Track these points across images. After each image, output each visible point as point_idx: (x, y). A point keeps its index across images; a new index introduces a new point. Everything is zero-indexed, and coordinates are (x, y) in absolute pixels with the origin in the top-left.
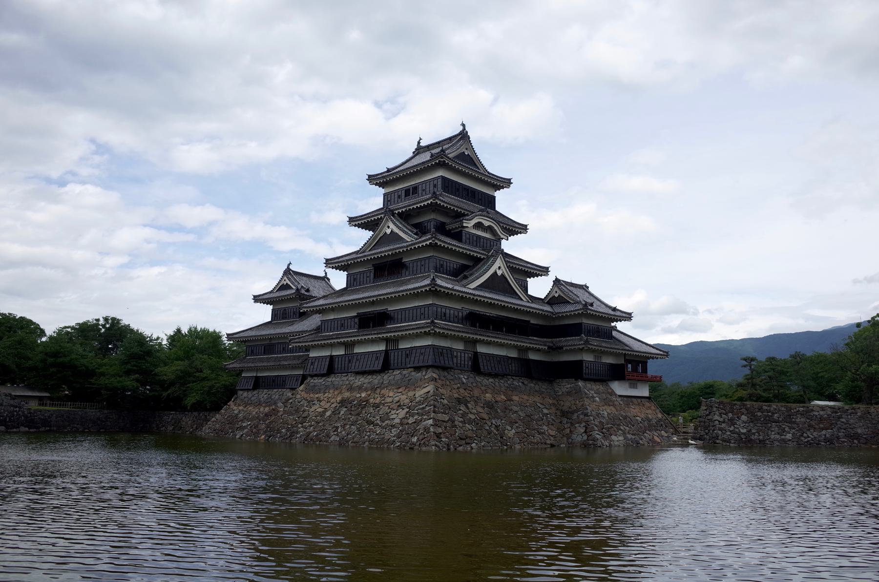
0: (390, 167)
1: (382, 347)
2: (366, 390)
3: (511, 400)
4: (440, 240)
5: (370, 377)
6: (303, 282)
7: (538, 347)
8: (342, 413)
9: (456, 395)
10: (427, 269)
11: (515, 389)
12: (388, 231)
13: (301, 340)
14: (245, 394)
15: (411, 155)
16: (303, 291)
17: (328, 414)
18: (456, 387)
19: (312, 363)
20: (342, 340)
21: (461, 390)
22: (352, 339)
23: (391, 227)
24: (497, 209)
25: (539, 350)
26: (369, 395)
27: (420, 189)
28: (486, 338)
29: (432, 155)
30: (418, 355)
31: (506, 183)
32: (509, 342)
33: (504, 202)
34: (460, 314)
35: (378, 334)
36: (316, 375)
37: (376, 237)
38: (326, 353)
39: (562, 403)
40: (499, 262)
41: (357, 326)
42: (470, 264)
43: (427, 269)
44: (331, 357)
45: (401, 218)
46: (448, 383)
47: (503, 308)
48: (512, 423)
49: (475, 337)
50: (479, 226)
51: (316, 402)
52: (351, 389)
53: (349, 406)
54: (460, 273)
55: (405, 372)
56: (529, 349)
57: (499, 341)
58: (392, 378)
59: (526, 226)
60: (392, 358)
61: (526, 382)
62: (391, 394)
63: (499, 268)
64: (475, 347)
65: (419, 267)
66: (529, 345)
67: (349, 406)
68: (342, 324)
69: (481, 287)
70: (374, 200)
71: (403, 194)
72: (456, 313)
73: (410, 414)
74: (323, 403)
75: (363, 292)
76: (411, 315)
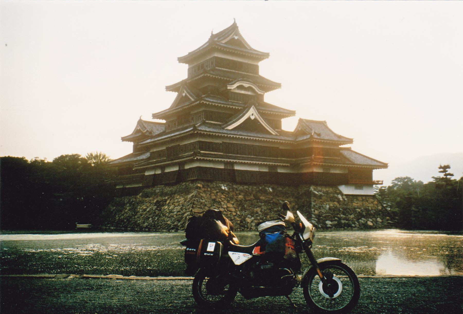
3: (259, 199)
4: (205, 100)
9: (214, 197)
12: (184, 94)
14: (118, 199)
18: (215, 192)
21: (218, 194)
25: (288, 166)
28: (238, 161)
31: (263, 56)
38: (152, 173)
39: (300, 200)
44: (155, 175)
46: (209, 189)
48: (252, 214)
50: (240, 87)
55: (187, 183)
56: (277, 165)
62: (178, 198)
63: (253, 115)
64: (233, 167)
68: (160, 154)
73: (182, 209)
74: (147, 204)
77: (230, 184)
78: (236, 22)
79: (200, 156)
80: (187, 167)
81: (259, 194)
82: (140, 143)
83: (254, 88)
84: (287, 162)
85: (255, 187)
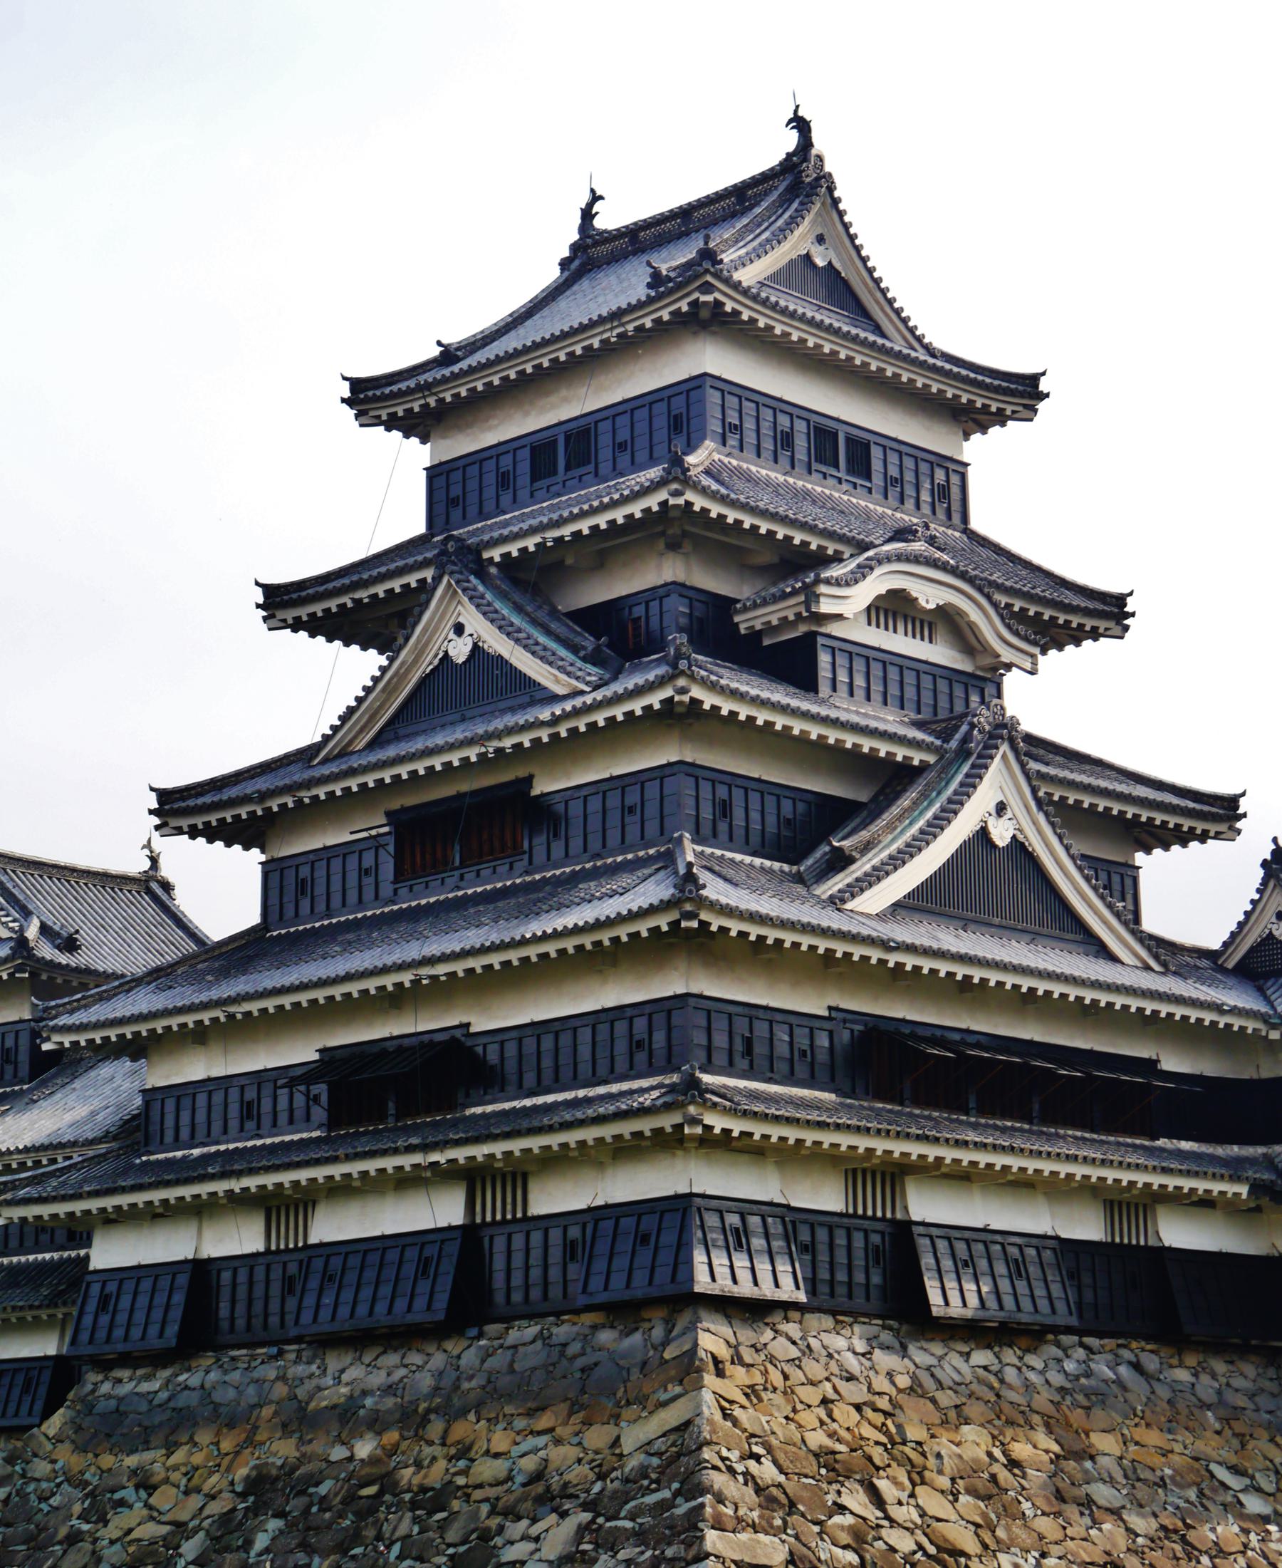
0: (454, 336)
1: (445, 1210)
2: (376, 1424)
4: (713, 687)
5: (392, 1359)
6: (49, 905)
7: (1201, 1185)
8: (261, 1541)
9: (817, 1439)
10: (652, 828)
11: (1097, 1398)
12: (460, 650)
13: (50, 1187)
15: (552, 274)
16: (46, 951)
17: (190, 1548)
19: (104, 1301)
20: (252, 1183)
22: (303, 1175)
23: (463, 627)
24: (976, 524)
25: (1206, 1203)
26: (393, 1451)
27: (605, 440)
28: (949, 1154)
29: (657, 279)
30: (625, 1245)
31: (1023, 393)
32: (1064, 1169)
33: (1016, 490)
34: (823, 1041)
35: (425, 1148)
36: (127, 1360)
37: (401, 677)
40: (997, 782)
41: (319, 1114)
42: (863, 796)
43: (652, 828)
44: (200, 1269)
45: (516, 582)
46: (776, 1377)
47: (1027, 1002)
49: (898, 1148)
51: (128, 1493)
52: (299, 1420)
53: (295, 1506)
54: (809, 835)
55: (562, 1332)
57: (1015, 1162)
58: (496, 1362)
59: (1120, 600)
60: (499, 1263)
61: (1151, 1363)
62: (500, 1441)
63: (1001, 808)
65: (614, 820)
66: (1156, 1180)
67: (295, 1506)
69: (918, 904)
70: (378, 495)
71: (524, 467)
72: (803, 1042)
75: (348, 947)
76: (585, 1052)
77: (886, 1337)
78: (820, 142)
79: (726, 1111)
80: (554, 1198)
81: (1077, 1417)
82: (64, 1020)
83: (974, 615)
84: (1234, 1170)
85: (1035, 1361)
